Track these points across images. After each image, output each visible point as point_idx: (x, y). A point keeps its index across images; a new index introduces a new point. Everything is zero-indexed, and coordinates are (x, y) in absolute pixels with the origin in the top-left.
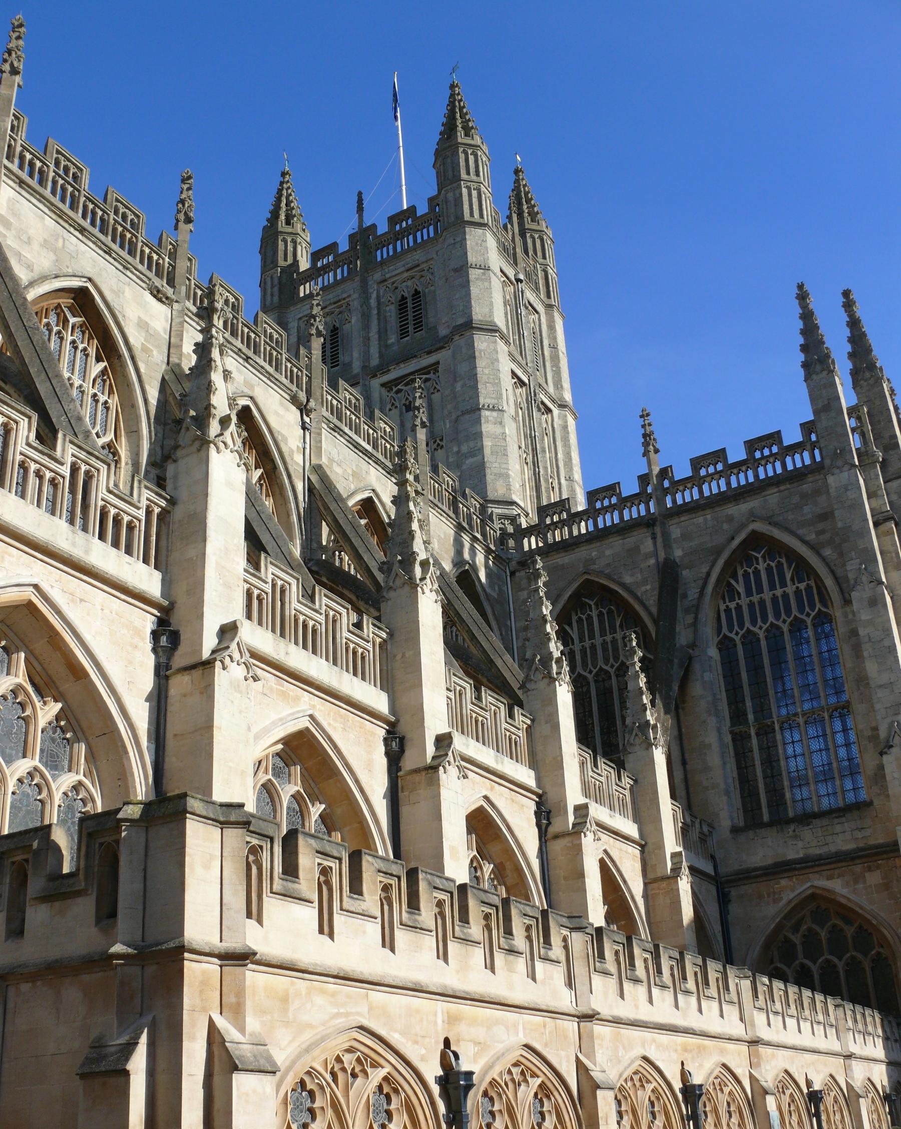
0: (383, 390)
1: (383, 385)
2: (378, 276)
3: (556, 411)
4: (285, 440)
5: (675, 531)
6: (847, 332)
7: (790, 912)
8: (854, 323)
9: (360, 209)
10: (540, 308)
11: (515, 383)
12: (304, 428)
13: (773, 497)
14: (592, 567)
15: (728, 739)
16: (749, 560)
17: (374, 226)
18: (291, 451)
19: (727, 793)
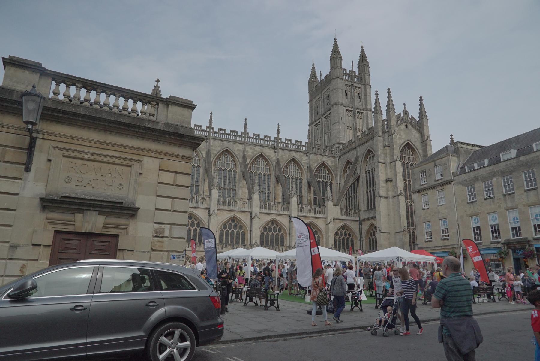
0: (325, 119)
1: (324, 118)
2: (323, 92)
3: (364, 112)
4: (270, 156)
5: (359, 149)
6: (387, 99)
7: (370, 227)
8: (389, 97)
9: (321, 75)
10: (362, 86)
11: (349, 112)
12: (275, 152)
13: (371, 142)
14: (349, 157)
15: (365, 192)
16: (370, 154)
17: (323, 79)
18: (272, 158)
19: (364, 204)
